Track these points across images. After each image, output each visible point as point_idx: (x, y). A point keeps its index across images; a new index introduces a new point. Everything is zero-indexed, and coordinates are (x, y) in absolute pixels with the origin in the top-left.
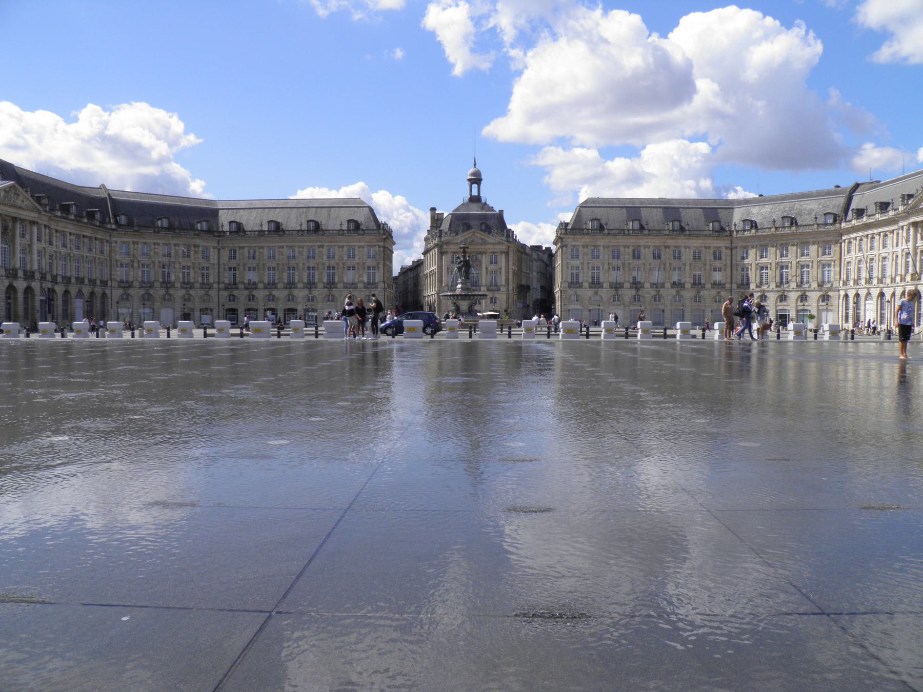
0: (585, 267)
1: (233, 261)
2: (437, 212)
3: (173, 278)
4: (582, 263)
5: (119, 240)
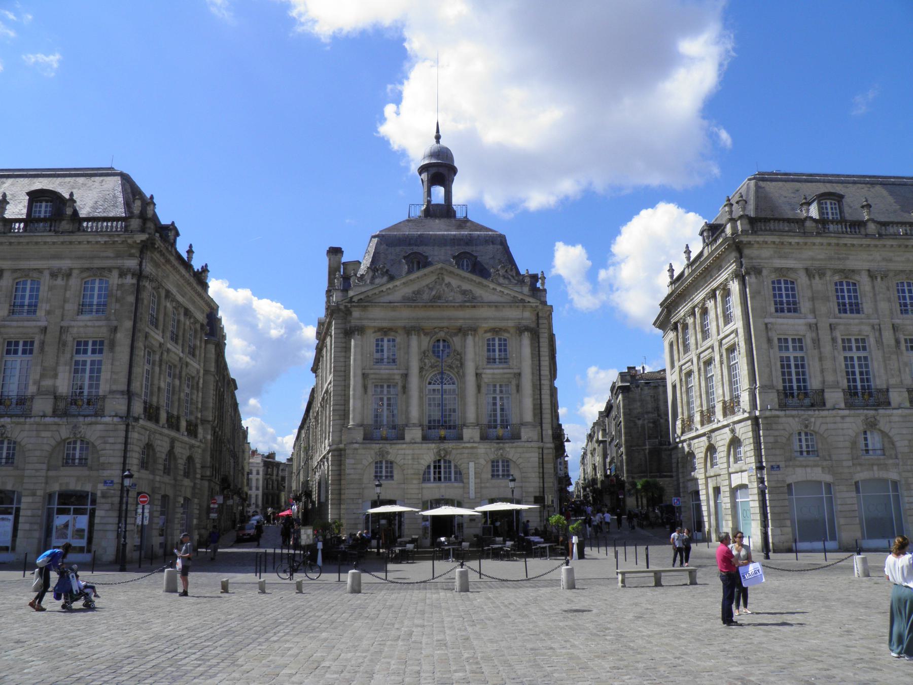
0: (825, 336)
2: (344, 259)
4: (813, 327)
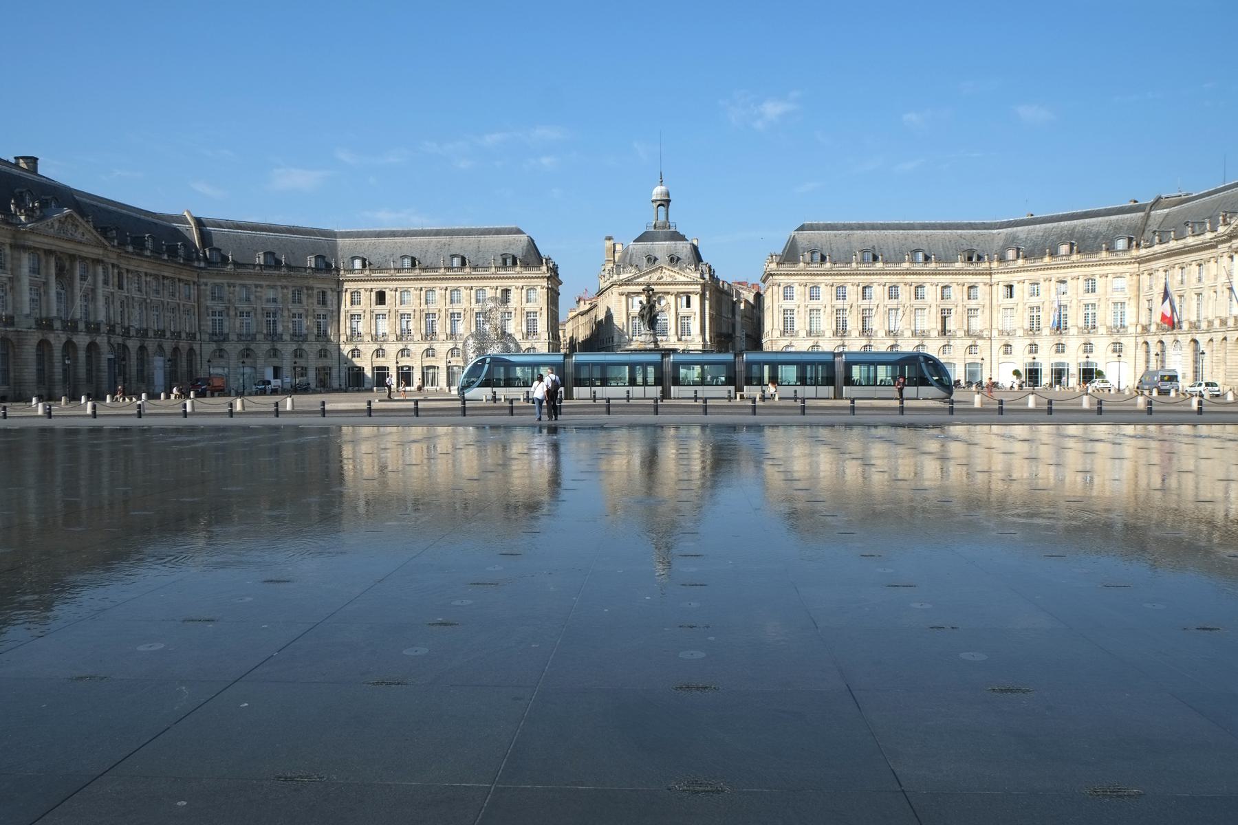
0: (802, 309)
1: (356, 307)
3: (280, 329)
5: (210, 281)
